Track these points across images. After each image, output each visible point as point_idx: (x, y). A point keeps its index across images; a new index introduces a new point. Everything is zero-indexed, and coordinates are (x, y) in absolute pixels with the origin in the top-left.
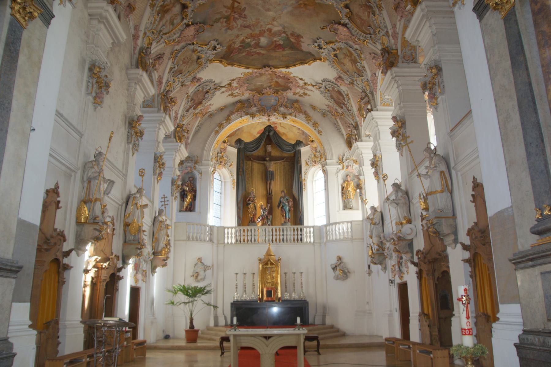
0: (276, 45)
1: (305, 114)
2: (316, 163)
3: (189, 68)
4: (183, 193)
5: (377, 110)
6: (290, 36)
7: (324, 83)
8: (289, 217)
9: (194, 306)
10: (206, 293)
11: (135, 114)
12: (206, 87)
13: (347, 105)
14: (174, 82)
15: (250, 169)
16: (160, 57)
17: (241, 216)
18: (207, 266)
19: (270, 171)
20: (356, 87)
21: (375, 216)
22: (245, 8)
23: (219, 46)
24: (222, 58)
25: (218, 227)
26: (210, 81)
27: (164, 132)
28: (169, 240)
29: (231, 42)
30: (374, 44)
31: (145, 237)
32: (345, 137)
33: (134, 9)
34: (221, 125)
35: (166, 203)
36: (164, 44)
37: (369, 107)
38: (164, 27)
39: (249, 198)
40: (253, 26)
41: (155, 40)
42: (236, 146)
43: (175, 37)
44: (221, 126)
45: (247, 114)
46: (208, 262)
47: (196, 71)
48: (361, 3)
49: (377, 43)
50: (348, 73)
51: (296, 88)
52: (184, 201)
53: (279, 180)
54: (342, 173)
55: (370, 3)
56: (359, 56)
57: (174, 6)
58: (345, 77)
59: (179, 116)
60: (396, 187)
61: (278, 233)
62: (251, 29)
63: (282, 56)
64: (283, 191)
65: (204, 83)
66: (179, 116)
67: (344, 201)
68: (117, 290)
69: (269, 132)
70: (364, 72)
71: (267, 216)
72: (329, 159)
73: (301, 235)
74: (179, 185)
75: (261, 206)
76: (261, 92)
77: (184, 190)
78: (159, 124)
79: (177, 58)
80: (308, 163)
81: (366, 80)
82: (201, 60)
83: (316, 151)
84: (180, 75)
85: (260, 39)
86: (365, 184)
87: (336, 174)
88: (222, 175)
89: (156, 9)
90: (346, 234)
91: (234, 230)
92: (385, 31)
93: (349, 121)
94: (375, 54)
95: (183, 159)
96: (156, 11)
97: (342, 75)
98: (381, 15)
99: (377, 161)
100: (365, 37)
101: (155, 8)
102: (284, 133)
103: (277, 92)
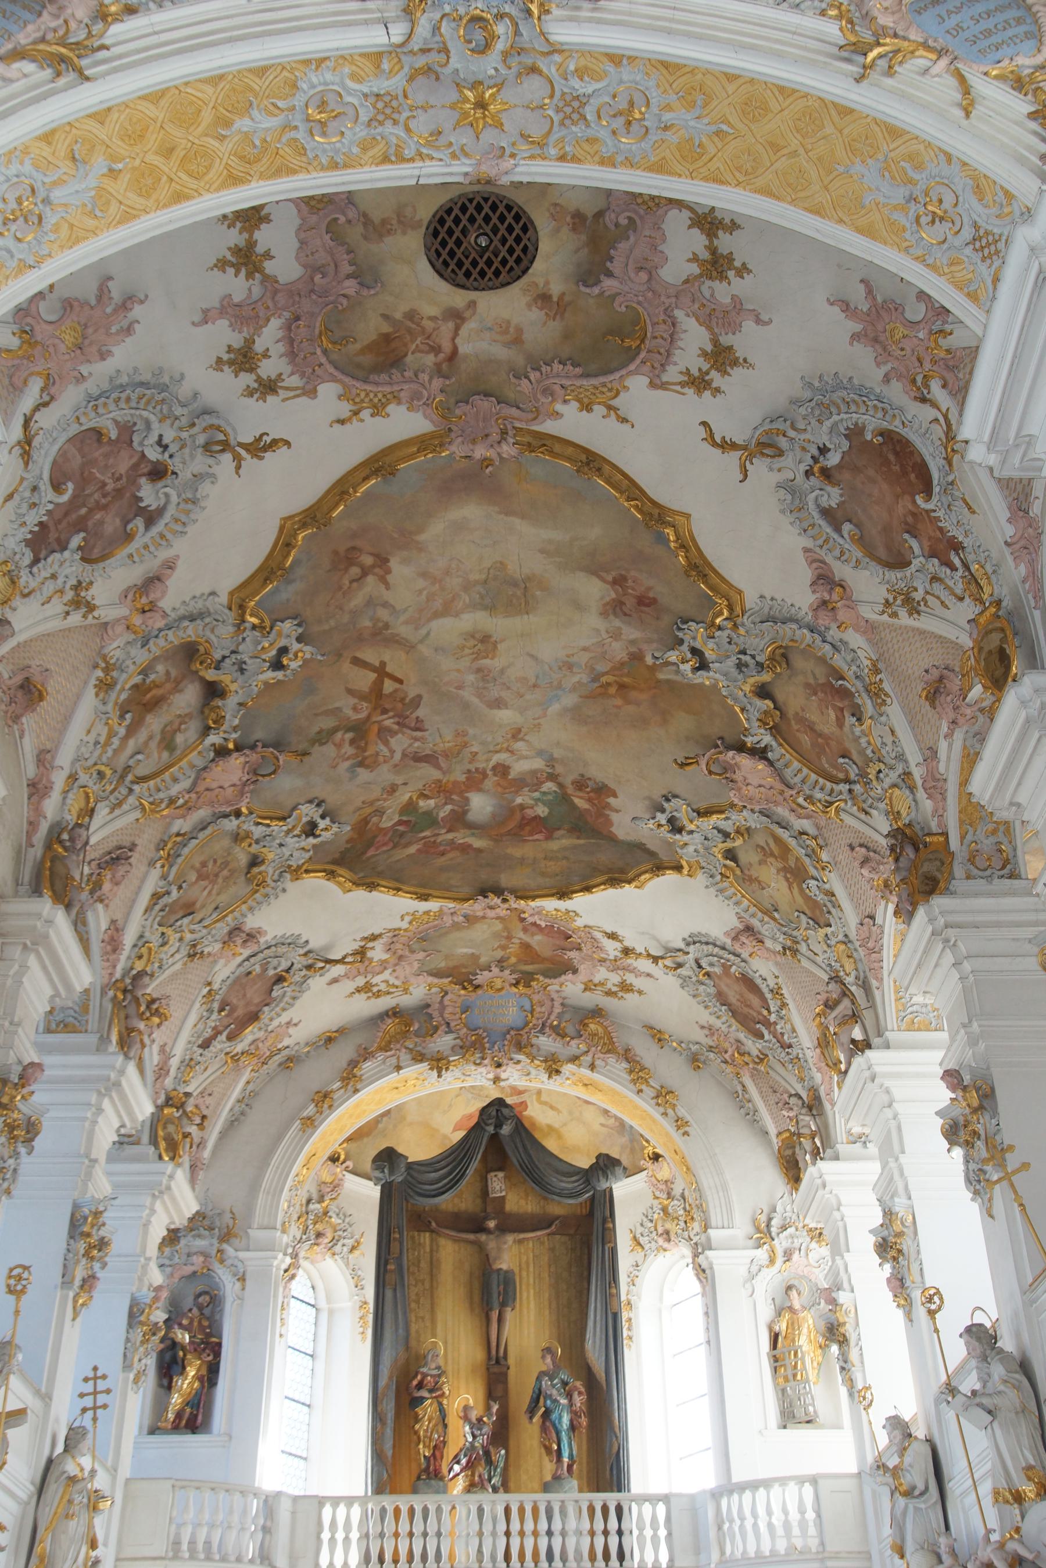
0: (523, 818)
2: (669, 1240)
3: (218, 894)
4: (168, 1356)
5: (887, 1046)
6: (570, 790)
7: (692, 948)
8: (571, 1456)
11: (12, 1059)
12: (275, 962)
13: (778, 1027)
14: (163, 944)
15: (424, 1265)
16: (118, 858)
17: (390, 1453)
20: (805, 963)
21: (908, 1459)
22: (419, 697)
23: (327, 821)
24: (336, 862)
25: (296, 1499)
26: (291, 942)
27: (117, 1125)
29: (369, 810)
30: (863, 816)
32: (776, 1142)
33: (41, 698)
34: (326, 1096)
35: (101, 1399)
36: (137, 814)
37: (857, 1034)
38: (140, 757)
39: (419, 1377)
40: (446, 755)
41: (107, 798)
42: (377, 1174)
43: (175, 790)
44: (324, 1099)
45: (419, 1057)
47: (244, 907)
48: (812, 681)
49: (874, 812)
50: (776, 914)
51: (594, 966)
52: (169, 1388)
53: (532, 1305)
54: (769, 1281)
55: (843, 678)
56: (812, 854)
57: (177, 689)
58: (767, 929)
59: (174, 1062)
60: (979, 1339)
61: (529, 1526)
62: (438, 767)
63: (545, 858)
64: (548, 1350)
65: (269, 948)
66: (174, 1062)
67: (784, 1391)
69: (499, 1125)
70: (833, 910)
71: (487, 1453)
72: (720, 1224)
73: (620, 1533)
75: (466, 1408)
76: (470, 982)
78: (99, 1093)
79: (179, 860)
80: (642, 1240)
81: (841, 937)
82: (262, 868)
83: (670, 1196)
84: (186, 921)
85: (467, 799)
86: (857, 1324)
87: (745, 1282)
88: (320, 1286)
89: (118, 697)
90: (796, 1531)
91: (356, 1511)
92: (901, 771)
93: (783, 1083)
94: (868, 848)
95: (180, 1222)
96: (116, 703)
97: (755, 923)
98: (883, 719)
99: (900, 1234)
100: (832, 790)
101: (113, 695)
102: (551, 1129)
103: (525, 980)
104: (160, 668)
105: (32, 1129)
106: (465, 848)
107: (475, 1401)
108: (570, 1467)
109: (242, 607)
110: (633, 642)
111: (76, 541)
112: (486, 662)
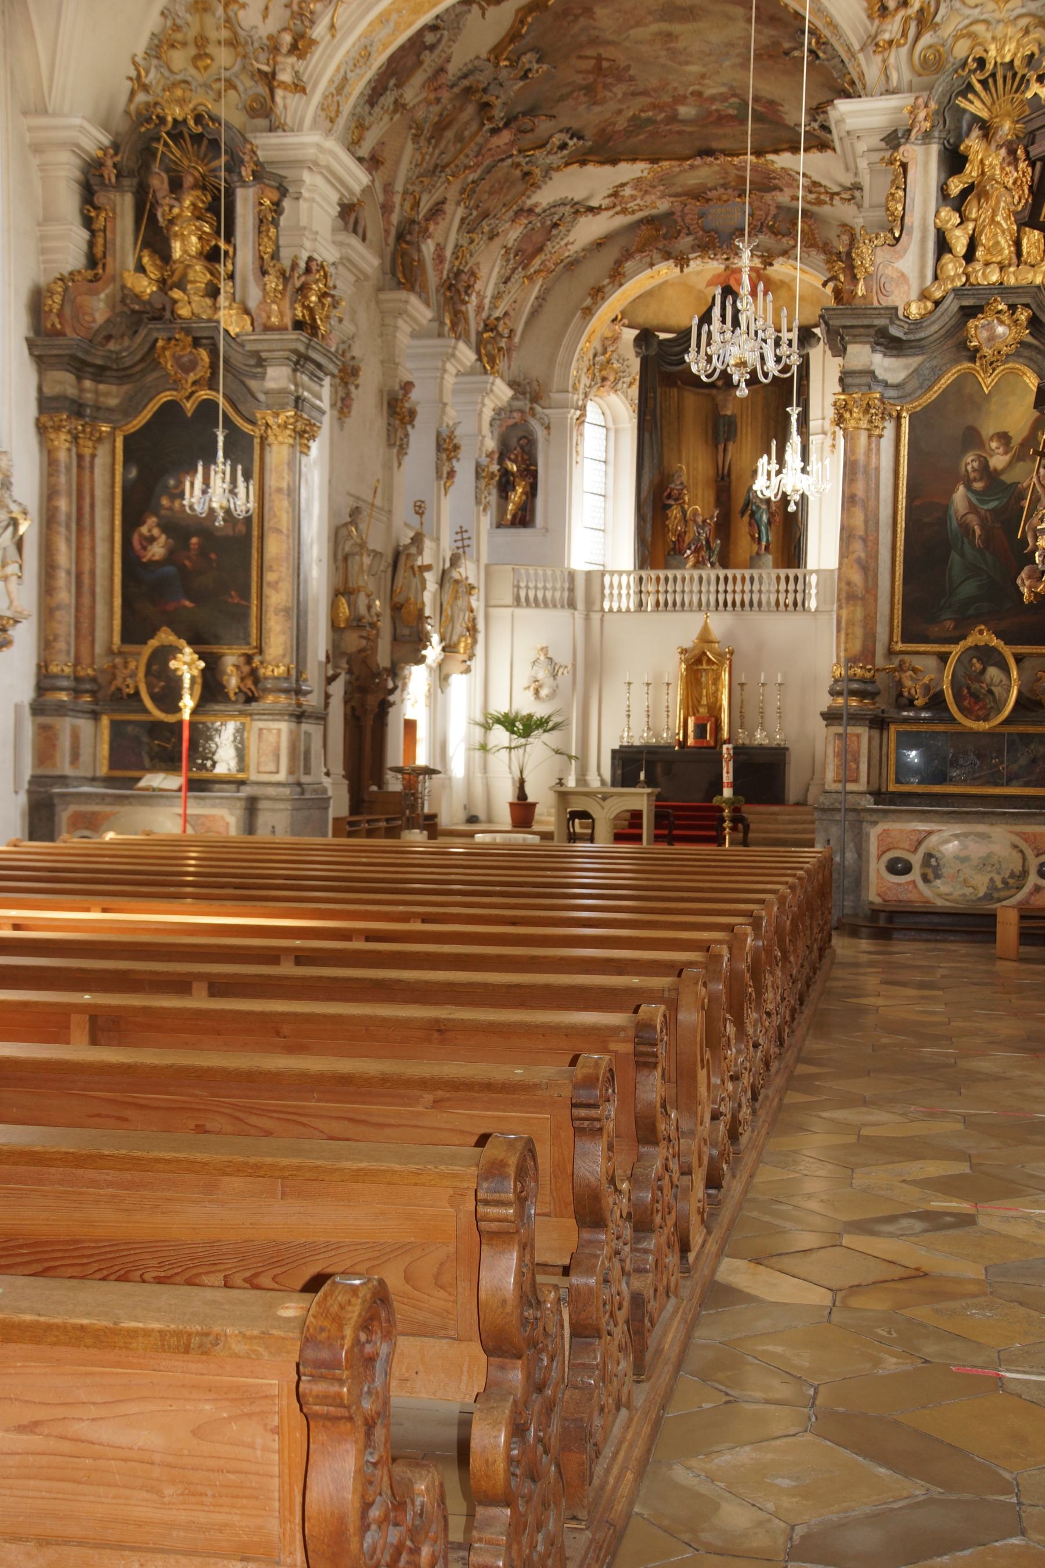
1: (825, 252)
4: (504, 480)
8: (768, 541)
9: (527, 756)
10: (553, 729)
14: (472, 241)
17: (649, 539)
18: (560, 667)
19: (725, 416)
23: (575, 140)
28: (474, 619)
31: (429, 627)
35: (466, 542)
36: (446, 185)
40: (655, 90)
44: (598, 294)
45: (667, 256)
46: (563, 657)
57: (462, 109)
59: (487, 301)
65: (544, 211)
66: (487, 301)
68: (386, 725)
74: (493, 473)
77: (505, 473)
84: (484, 223)
104: (449, 107)
105: (412, 414)
106: (680, 133)
107: (702, 508)
108: (767, 548)
109: (497, 58)
110: (773, 36)
111: (392, 82)
112: (673, 45)
